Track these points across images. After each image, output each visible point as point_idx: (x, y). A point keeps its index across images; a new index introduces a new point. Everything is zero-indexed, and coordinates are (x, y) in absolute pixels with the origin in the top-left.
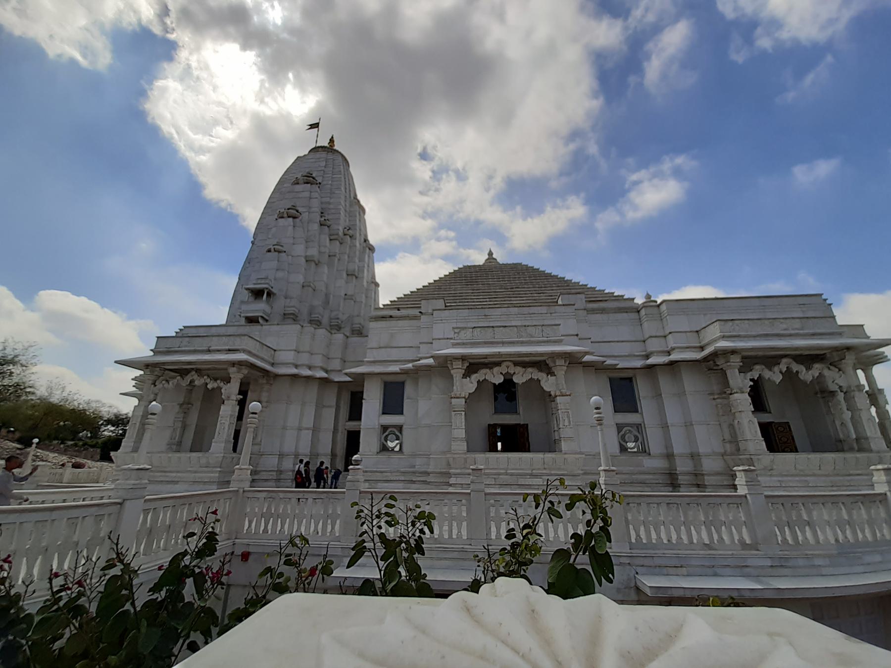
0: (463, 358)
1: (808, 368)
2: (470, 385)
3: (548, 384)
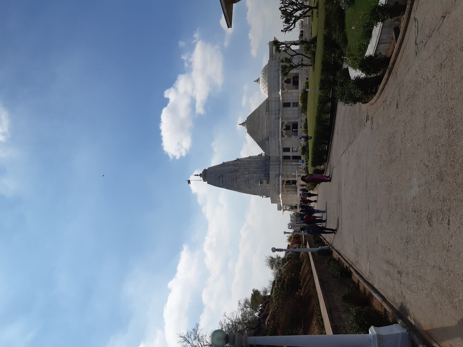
2: (286, 136)
3: (286, 123)
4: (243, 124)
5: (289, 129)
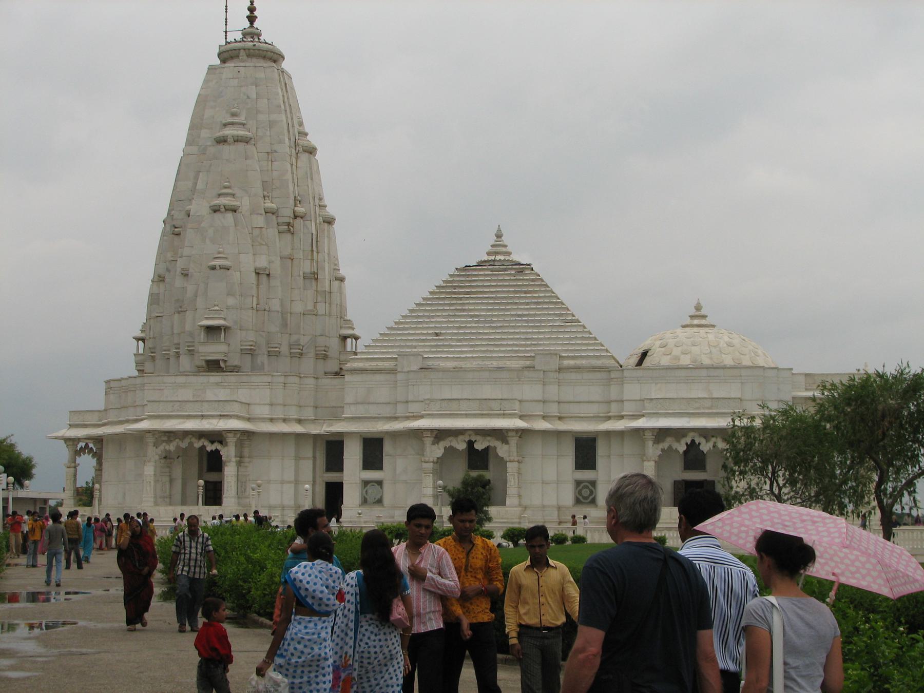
0: (431, 430)
1: (707, 441)
2: (437, 451)
3: (502, 450)
4: (498, 246)
5: (472, 466)
